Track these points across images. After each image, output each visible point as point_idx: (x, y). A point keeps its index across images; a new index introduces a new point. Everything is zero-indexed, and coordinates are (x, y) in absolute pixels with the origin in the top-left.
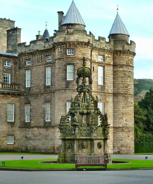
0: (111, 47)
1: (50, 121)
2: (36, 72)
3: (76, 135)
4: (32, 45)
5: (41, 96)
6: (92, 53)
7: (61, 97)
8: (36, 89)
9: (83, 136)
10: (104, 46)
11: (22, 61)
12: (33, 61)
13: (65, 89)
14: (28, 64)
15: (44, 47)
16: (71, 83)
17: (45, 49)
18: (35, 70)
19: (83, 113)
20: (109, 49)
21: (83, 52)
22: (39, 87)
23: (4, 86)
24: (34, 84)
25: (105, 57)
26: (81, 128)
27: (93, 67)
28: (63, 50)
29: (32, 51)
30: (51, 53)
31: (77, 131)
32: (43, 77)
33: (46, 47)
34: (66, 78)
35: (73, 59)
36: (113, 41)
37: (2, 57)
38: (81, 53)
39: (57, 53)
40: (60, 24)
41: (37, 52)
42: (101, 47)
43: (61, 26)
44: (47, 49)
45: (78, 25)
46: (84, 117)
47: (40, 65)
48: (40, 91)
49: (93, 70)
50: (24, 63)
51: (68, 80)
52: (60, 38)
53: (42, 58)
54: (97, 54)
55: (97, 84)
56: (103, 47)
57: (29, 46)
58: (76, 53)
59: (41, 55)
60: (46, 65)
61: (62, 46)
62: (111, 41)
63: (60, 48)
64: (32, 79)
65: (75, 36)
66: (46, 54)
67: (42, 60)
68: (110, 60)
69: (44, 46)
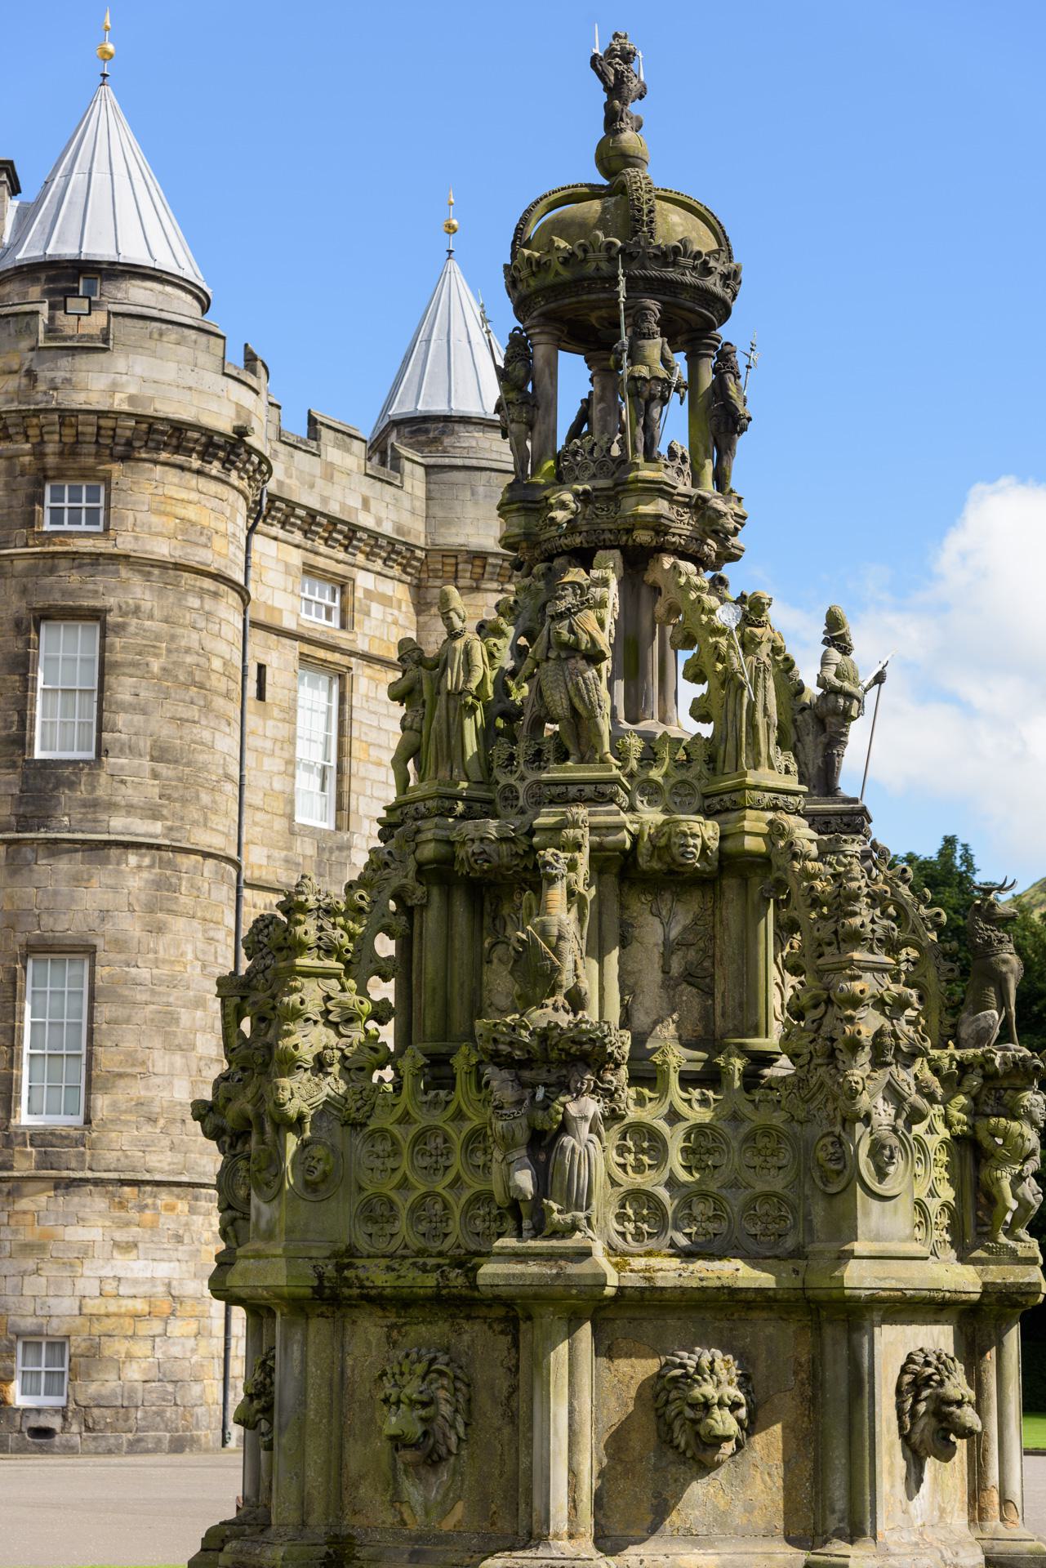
0: (406, 519)
6: (257, 540)
10: (355, 502)
20: (387, 529)
21: (191, 513)
25: (359, 594)
27: (261, 668)
34: (22, 742)
36: (420, 471)
38: (172, 523)
42: (325, 500)
45: (149, 284)
49: (261, 695)
51: (38, 754)
54: (296, 557)
55: (291, 817)
56: (343, 505)
58: (122, 519)
62: (407, 465)
68: (395, 623)
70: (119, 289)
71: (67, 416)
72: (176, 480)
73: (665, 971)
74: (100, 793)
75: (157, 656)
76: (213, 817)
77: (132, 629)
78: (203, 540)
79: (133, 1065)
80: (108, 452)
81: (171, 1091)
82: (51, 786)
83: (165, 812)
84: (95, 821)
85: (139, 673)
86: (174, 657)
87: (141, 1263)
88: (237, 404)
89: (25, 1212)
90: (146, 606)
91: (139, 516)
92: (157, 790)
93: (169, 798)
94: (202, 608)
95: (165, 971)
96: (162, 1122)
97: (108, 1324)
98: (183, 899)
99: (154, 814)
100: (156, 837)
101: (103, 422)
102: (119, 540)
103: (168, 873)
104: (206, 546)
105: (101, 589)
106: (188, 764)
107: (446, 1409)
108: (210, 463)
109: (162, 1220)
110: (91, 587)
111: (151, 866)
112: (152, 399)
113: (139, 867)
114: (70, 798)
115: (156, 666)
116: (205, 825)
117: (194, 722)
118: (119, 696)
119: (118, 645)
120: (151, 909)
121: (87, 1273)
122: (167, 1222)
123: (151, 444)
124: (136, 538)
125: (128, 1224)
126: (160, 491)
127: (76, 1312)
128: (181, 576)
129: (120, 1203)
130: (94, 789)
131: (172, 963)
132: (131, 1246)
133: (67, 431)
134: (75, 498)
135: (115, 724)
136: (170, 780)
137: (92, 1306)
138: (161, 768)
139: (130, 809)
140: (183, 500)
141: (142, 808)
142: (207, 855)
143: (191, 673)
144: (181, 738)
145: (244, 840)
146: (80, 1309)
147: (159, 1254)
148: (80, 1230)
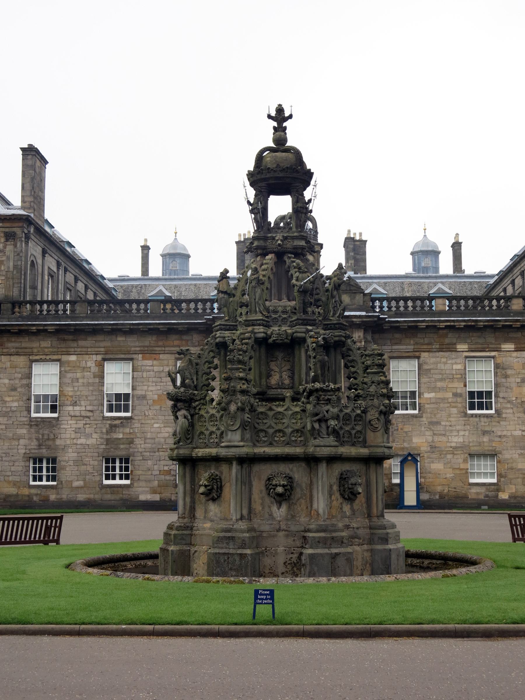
9: (207, 446)
26: (202, 412)
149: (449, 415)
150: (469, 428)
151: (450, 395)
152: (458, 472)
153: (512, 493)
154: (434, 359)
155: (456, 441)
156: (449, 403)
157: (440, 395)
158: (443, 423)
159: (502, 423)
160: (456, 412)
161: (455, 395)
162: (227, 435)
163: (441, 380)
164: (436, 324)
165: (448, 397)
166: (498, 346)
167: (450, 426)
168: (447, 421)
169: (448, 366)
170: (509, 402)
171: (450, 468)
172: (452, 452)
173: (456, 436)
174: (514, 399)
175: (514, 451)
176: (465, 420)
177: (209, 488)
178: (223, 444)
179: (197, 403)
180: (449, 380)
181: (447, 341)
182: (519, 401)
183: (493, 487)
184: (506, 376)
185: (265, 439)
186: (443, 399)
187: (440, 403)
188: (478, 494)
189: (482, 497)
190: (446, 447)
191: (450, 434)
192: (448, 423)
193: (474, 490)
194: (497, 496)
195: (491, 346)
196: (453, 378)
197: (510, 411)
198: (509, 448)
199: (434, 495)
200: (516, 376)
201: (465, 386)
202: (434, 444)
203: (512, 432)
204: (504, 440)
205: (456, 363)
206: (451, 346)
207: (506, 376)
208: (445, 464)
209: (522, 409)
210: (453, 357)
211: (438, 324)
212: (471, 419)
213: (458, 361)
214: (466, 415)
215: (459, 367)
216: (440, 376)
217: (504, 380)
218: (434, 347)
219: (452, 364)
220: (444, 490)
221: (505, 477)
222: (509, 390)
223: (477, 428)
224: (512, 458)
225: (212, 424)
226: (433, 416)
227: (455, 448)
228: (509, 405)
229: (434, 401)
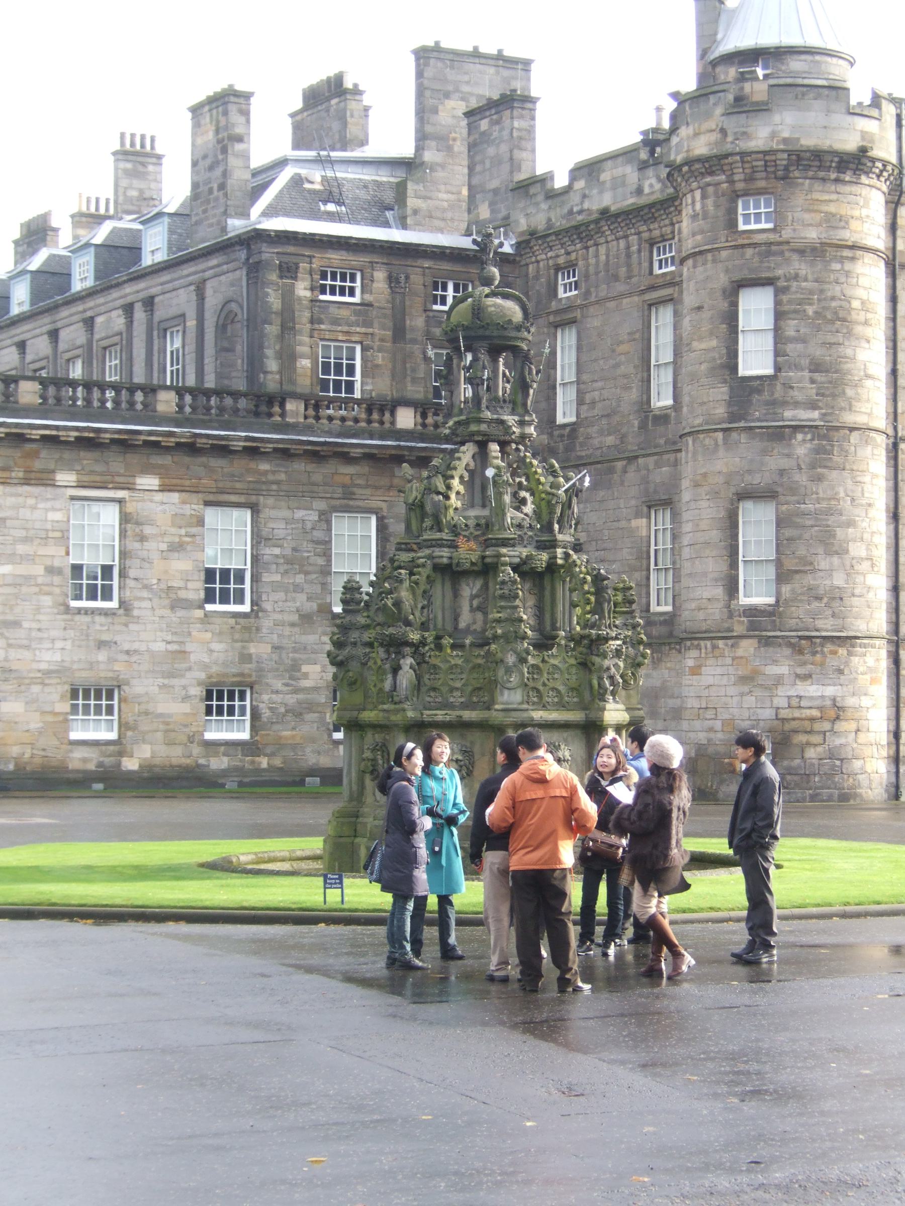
1: (669, 608)
2: (599, 335)
3: (400, 702)
4: (580, 184)
5: (625, 471)
7: (705, 475)
8: (601, 433)
11: (537, 277)
12: (587, 276)
13: (724, 430)
14: (569, 294)
15: (639, 191)
16: (759, 391)
17: (642, 201)
18: (596, 323)
19: (458, 564)
22: (616, 418)
23: (430, 420)
24: (593, 403)
26: (434, 661)
28: (717, 206)
29: (580, 218)
30: (673, 224)
31: (406, 676)
32: (637, 362)
33: (647, 190)
34: (734, 368)
35: (769, 253)
37: (420, 262)
38: (818, 217)
39: (686, 225)
40: (703, 54)
41: (603, 223)
43: (710, 69)
44: (651, 206)
45: (803, 57)
46: (469, 589)
47: (621, 296)
48: (622, 442)
50: (543, 291)
51: (743, 372)
52: (696, 134)
53: (629, 256)
57: (567, 190)
59: (626, 237)
60: (649, 296)
61: (708, 179)
63: (698, 194)
64: (585, 377)
65: (777, 118)
66: (650, 230)
67: (629, 265)
69: (635, 186)
70: (783, 64)
71: (743, 154)
72: (820, 188)
73: (471, 606)
74: (777, 395)
75: (810, 304)
76: (856, 404)
77: (793, 289)
78: (842, 224)
79: (805, 565)
80: (773, 176)
81: (832, 580)
82: (746, 394)
83: (820, 404)
84: (775, 413)
85: (799, 317)
86: (823, 304)
87: (814, 687)
88: (862, 131)
89: (741, 658)
90: (803, 273)
91: (796, 215)
92: (814, 391)
93: (823, 395)
94: (842, 269)
95: (824, 505)
96: (825, 600)
97: (794, 725)
98: (835, 459)
99: (813, 406)
100: (814, 420)
101: (767, 158)
102: (783, 232)
103: (825, 442)
104: (844, 228)
105: (772, 265)
106: (836, 372)
107: (380, 762)
108: (844, 173)
109: (828, 660)
110: (766, 264)
111: (812, 440)
112: (798, 139)
113: (804, 440)
114: (759, 400)
115: (810, 311)
116: (850, 410)
117: (839, 344)
118: (787, 333)
119: (785, 301)
120: (813, 466)
121: (780, 694)
122: (832, 662)
123: (800, 168)
124: (794, 230)
125: (804, 664)
126: (809, 197)
127: (774, 717)
128: (826, 251)
129: (799, 650)
130: (773, 394)
131: (830, 499)
132: (807, 677)
133: (747, 165)
134: (757, 206)
135: (785, 351)
136: (824, 383)
137: (784, 714)
138: (817, 376)
139: (796, 404)
140: (825, 201)
141: (804, 403)
142: (852, 429)
143: (836, 313)
144: (830, 356)
145: (900, 410)
146: (776, 715)
147: (827, 681)
148: (775, 668)
149: (38, 609)
150: (72, 635)
151: (39, 570)
152: (50, 718)
153: (145, 759)
154: (13, 499)
155: (48, 659)
156: (37, 585)
157: (22, 569)
158: (26, 625)
159: (132, 627)
160: (50, 604)
161: (51, 570)
162: (502, 694)
163: (26, 540)
164: (25, 431)
165: (36, 574)
166: (130, 480)
167: (39, 630)
168: (33, 620)
169: (38, 514)
170: (146, 587)
171: (36, 711)
172: (39, 681)
173: (48, 649)
174: (155, 581)
175: (151, 680)
176: (65, 620)
177: (462, 763)
178: (497, 707)
179: (427, 648)
180: (39, 541)
181: (38, 465)
182: (163, 586)
183: (111, 748)
184: (142, 538)
185: (535, 699)
186: (27, 577)
187: (20, 585)
188: (85, 760)
189: (91, 766)
190: (30, 671)
191: (38, 646)
192: (35, 625)
193: (79, 754)
194: (119, 764)
195: (118, 479)
196: (47, 538)
197: (146, 604)
198: (143, 674)
199: (6, 764)
200: (160, 539)
201: (68, 554)
202: (7, 665)
203: (150, 644)
204: (134, 658)
205: (54, 509)
206: (44, 476)
207: (142, 538)
208: (27, 703)
209: (167, 602)
210: (49, 496)
211: (28, 431)
212: (77, 618)
213: (58, 504)
214: (67, 609)
215: (58, 516)
216: (23, 533)
217: (137, 545)
218: (13, 474)
219: (47, 510)
220: (24, 754)
221: (134, 728)
222: (147, 565)
223: (87, 635)
224: (147, 693)
225: (452, 676)
226: (8, 611)
227: (48, 673)
228: (145, 594)
229: (11, 582)
